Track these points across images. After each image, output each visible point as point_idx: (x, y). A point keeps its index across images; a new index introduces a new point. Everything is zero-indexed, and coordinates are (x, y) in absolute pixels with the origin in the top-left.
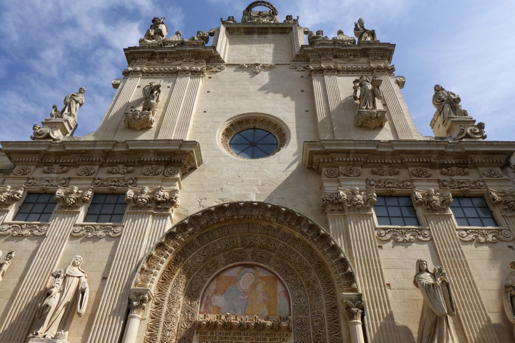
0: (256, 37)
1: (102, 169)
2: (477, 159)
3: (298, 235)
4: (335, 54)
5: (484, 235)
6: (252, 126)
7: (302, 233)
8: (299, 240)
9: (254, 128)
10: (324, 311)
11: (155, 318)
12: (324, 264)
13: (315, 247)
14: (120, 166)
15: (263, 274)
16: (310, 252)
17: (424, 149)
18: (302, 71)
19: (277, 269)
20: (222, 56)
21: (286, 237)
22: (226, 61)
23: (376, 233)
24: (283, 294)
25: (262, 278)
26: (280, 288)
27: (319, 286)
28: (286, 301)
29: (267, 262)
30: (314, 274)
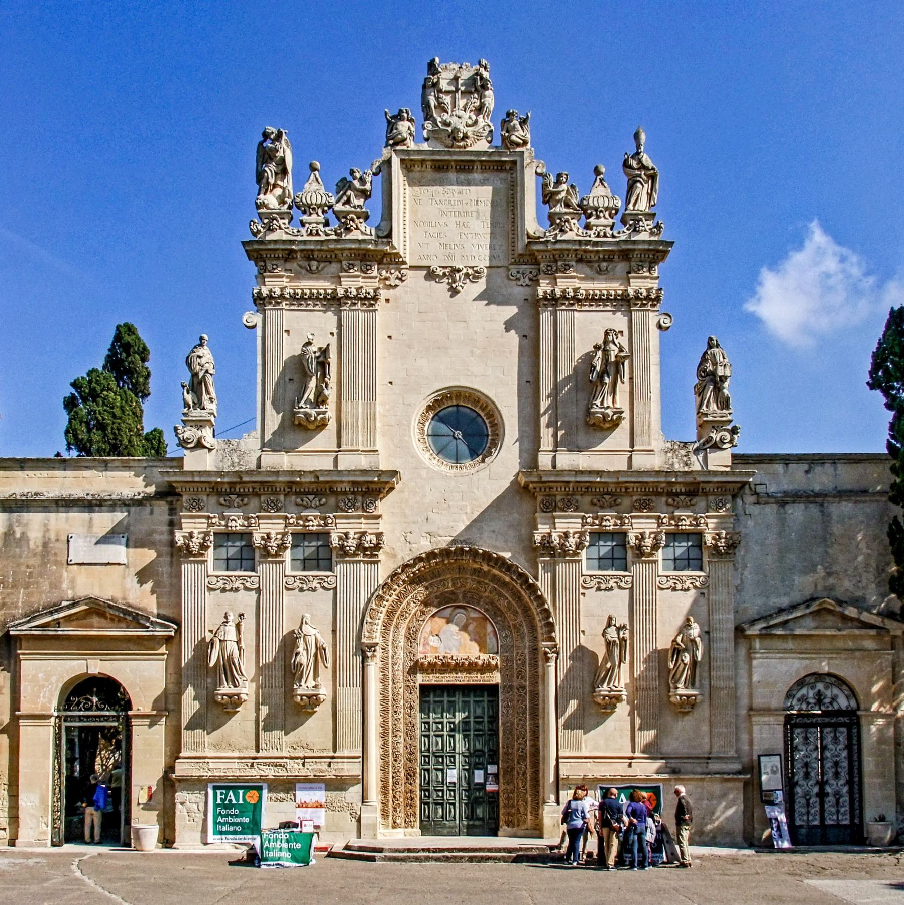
0: (452, 176)
1: (288, 499)
2: (708, 487)
3: (507, 579)
4: (579, 256)
5: (683, 582)
6: (454, 403)
7: (512, 579)
8: (508, 583)
9: (457, 406)
10: (527, 651)
11: (384, 659)
12: (530, 609)
13: (523, 593)
14: (311, 497)
15: (474, 615)
16: (518, 597)
17: (652, 480)
18: (527, 285)
19: (487, 610)
20: (402, 254)
21: (495, 579)
22: (407, 260)
23: (582, 579)
24: (492, 635)
25: (473, 619)
26: (489, 629)
27: (525, 629)
28: (494, 640)
29: (478, 604)
30: (521, 618)
